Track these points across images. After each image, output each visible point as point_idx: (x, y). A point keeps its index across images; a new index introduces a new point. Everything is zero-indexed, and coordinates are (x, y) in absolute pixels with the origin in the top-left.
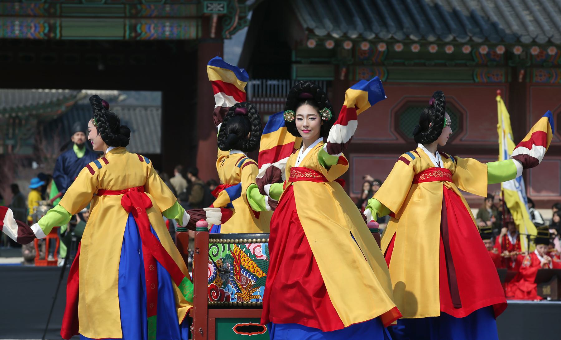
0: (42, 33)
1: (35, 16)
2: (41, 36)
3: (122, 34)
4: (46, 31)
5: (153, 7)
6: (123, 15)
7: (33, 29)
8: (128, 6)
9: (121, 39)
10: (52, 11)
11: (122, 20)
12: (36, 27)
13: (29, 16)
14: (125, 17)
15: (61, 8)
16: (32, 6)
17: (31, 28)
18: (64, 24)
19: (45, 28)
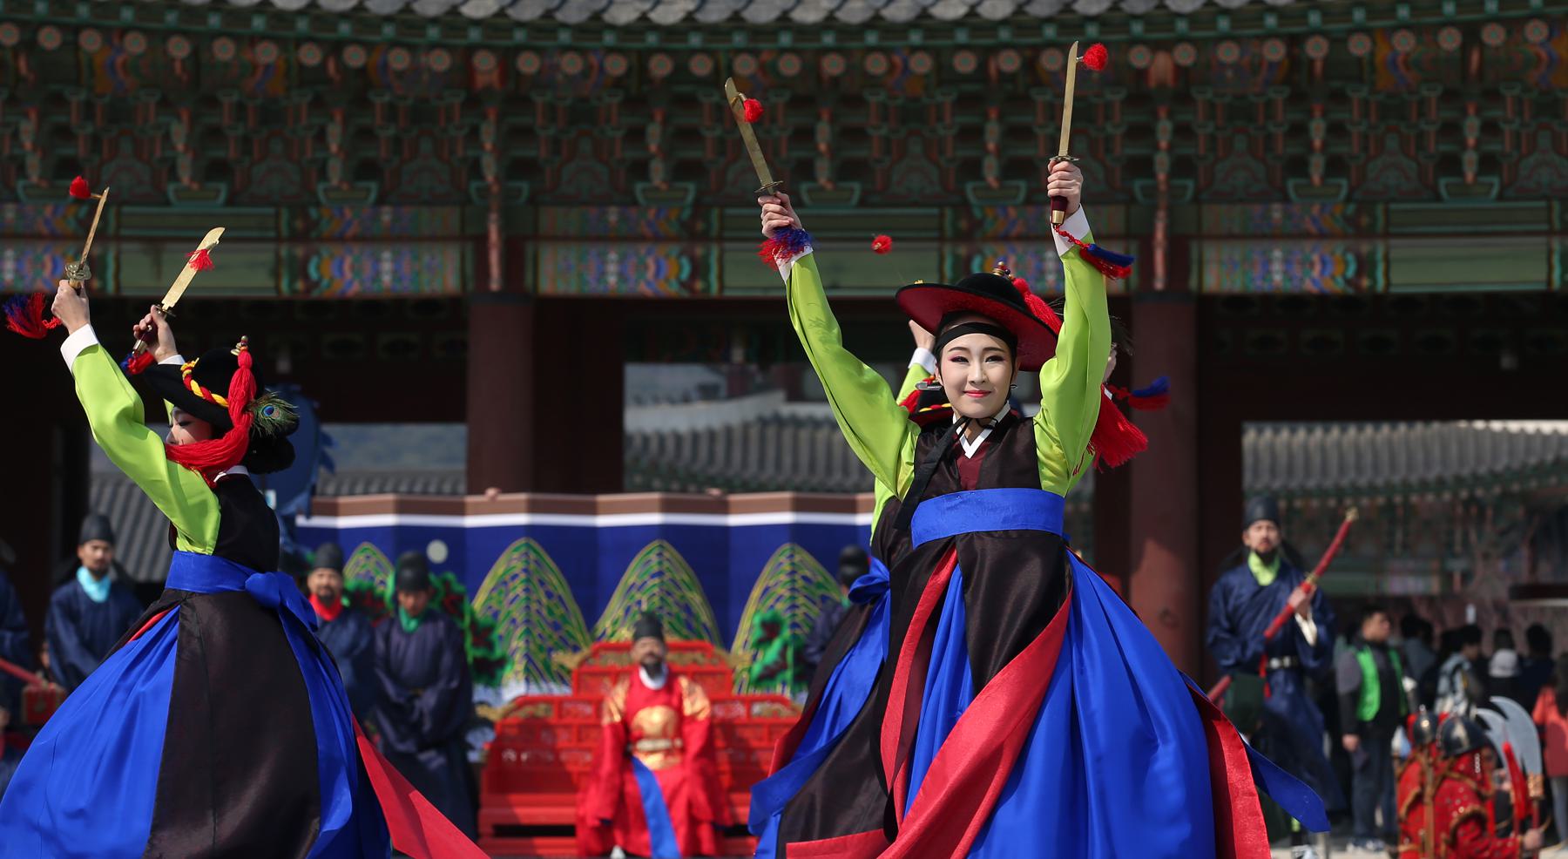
0: (1340, 280)
1: (1322, 236)
2: (1337, 286)
3: (1543, 276)
4: (1351, 272)
5: (348, 213)
6: (1544, 227)
7: (1318, 268)
8: (948, 212)
9: (1542, 287)
10: (1365, 220)
11: (1542, 240)
12: (1324, 263)
13: (1307, 236)
14: (1550, 233)
15: (1387, 212)
16: (1316, 210)
17: (1312, 265)
18: (1394, 254)
19: (1346, 263)
